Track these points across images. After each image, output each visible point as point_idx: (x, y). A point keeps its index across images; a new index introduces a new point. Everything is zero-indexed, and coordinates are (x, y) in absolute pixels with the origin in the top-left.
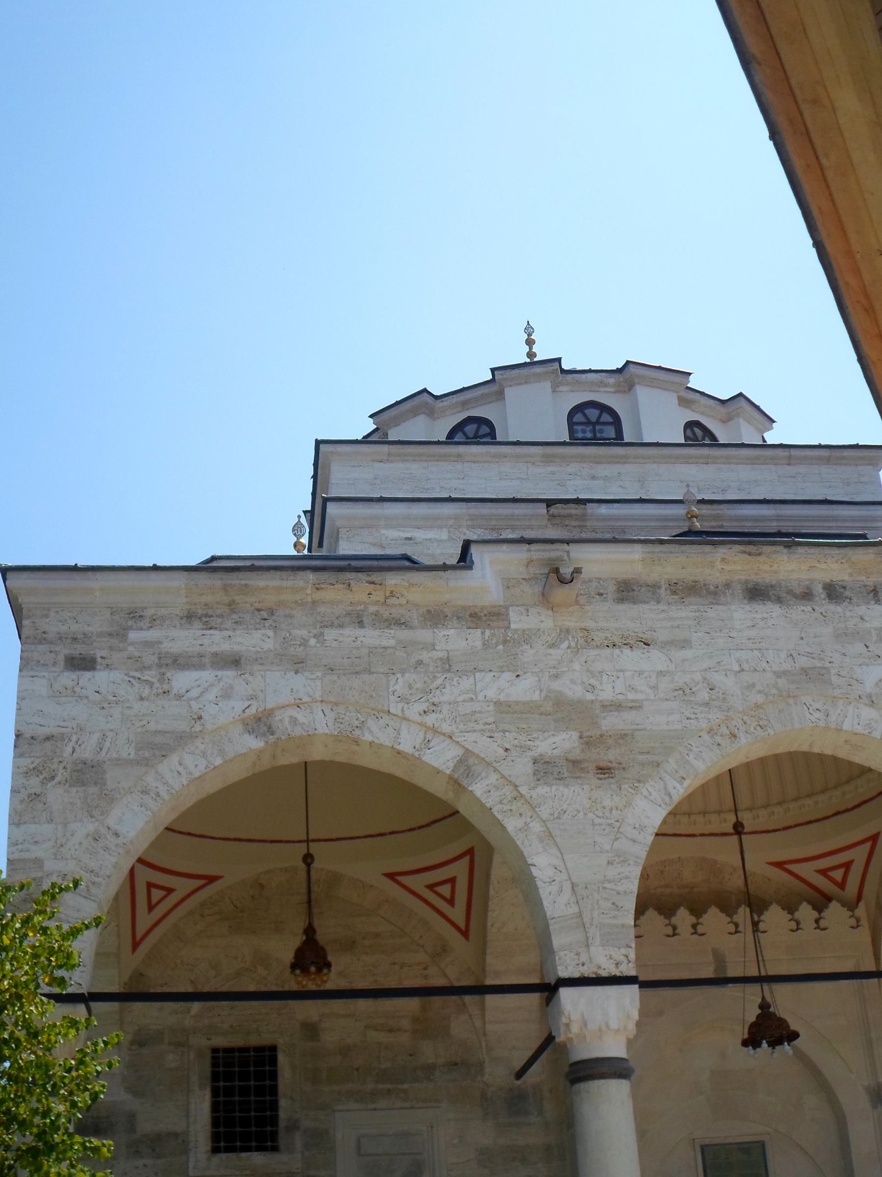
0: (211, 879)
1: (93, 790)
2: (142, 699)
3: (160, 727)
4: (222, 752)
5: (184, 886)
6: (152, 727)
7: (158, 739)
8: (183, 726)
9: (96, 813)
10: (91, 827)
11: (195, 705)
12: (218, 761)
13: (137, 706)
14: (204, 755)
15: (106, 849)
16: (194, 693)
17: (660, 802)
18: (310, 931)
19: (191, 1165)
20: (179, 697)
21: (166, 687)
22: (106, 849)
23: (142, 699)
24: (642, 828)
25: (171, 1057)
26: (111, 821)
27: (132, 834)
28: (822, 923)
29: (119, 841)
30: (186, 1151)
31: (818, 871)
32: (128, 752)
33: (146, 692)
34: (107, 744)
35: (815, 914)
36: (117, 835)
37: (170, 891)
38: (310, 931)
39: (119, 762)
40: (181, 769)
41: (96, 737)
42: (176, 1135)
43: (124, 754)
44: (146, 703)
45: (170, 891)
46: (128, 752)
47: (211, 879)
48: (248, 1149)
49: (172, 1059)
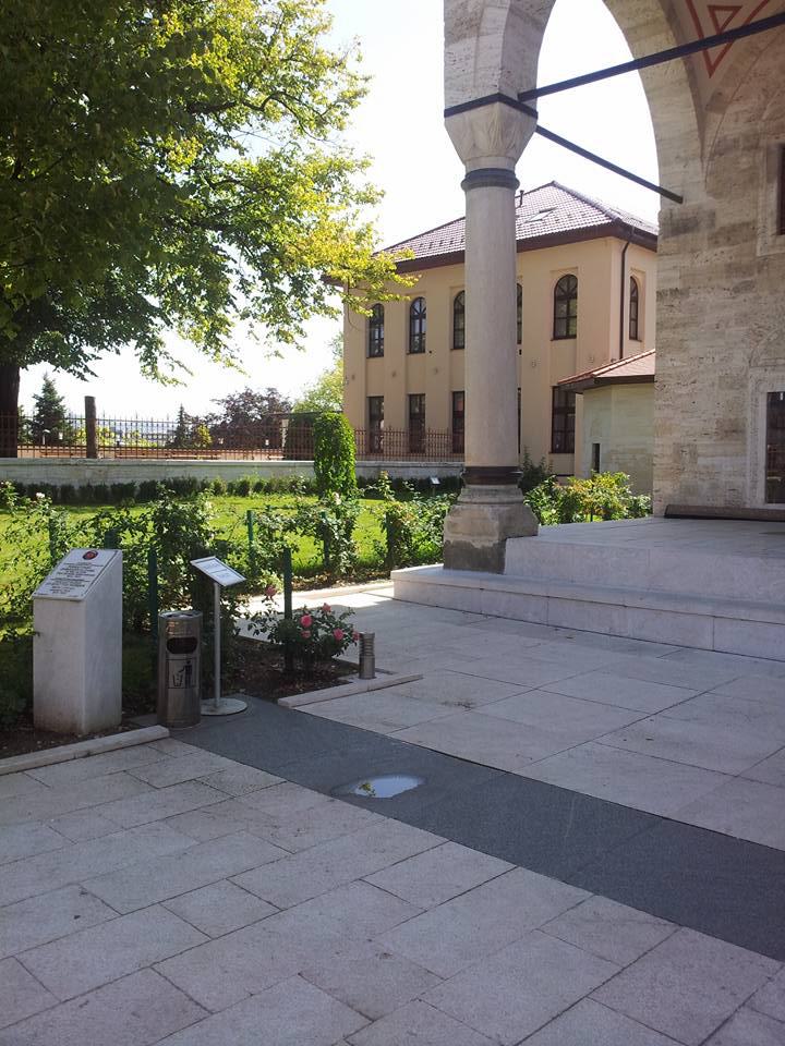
19: (758, 248)
25: (744, 160)
30: (754, 236)
42: (748, 224)
49: (745, 162)
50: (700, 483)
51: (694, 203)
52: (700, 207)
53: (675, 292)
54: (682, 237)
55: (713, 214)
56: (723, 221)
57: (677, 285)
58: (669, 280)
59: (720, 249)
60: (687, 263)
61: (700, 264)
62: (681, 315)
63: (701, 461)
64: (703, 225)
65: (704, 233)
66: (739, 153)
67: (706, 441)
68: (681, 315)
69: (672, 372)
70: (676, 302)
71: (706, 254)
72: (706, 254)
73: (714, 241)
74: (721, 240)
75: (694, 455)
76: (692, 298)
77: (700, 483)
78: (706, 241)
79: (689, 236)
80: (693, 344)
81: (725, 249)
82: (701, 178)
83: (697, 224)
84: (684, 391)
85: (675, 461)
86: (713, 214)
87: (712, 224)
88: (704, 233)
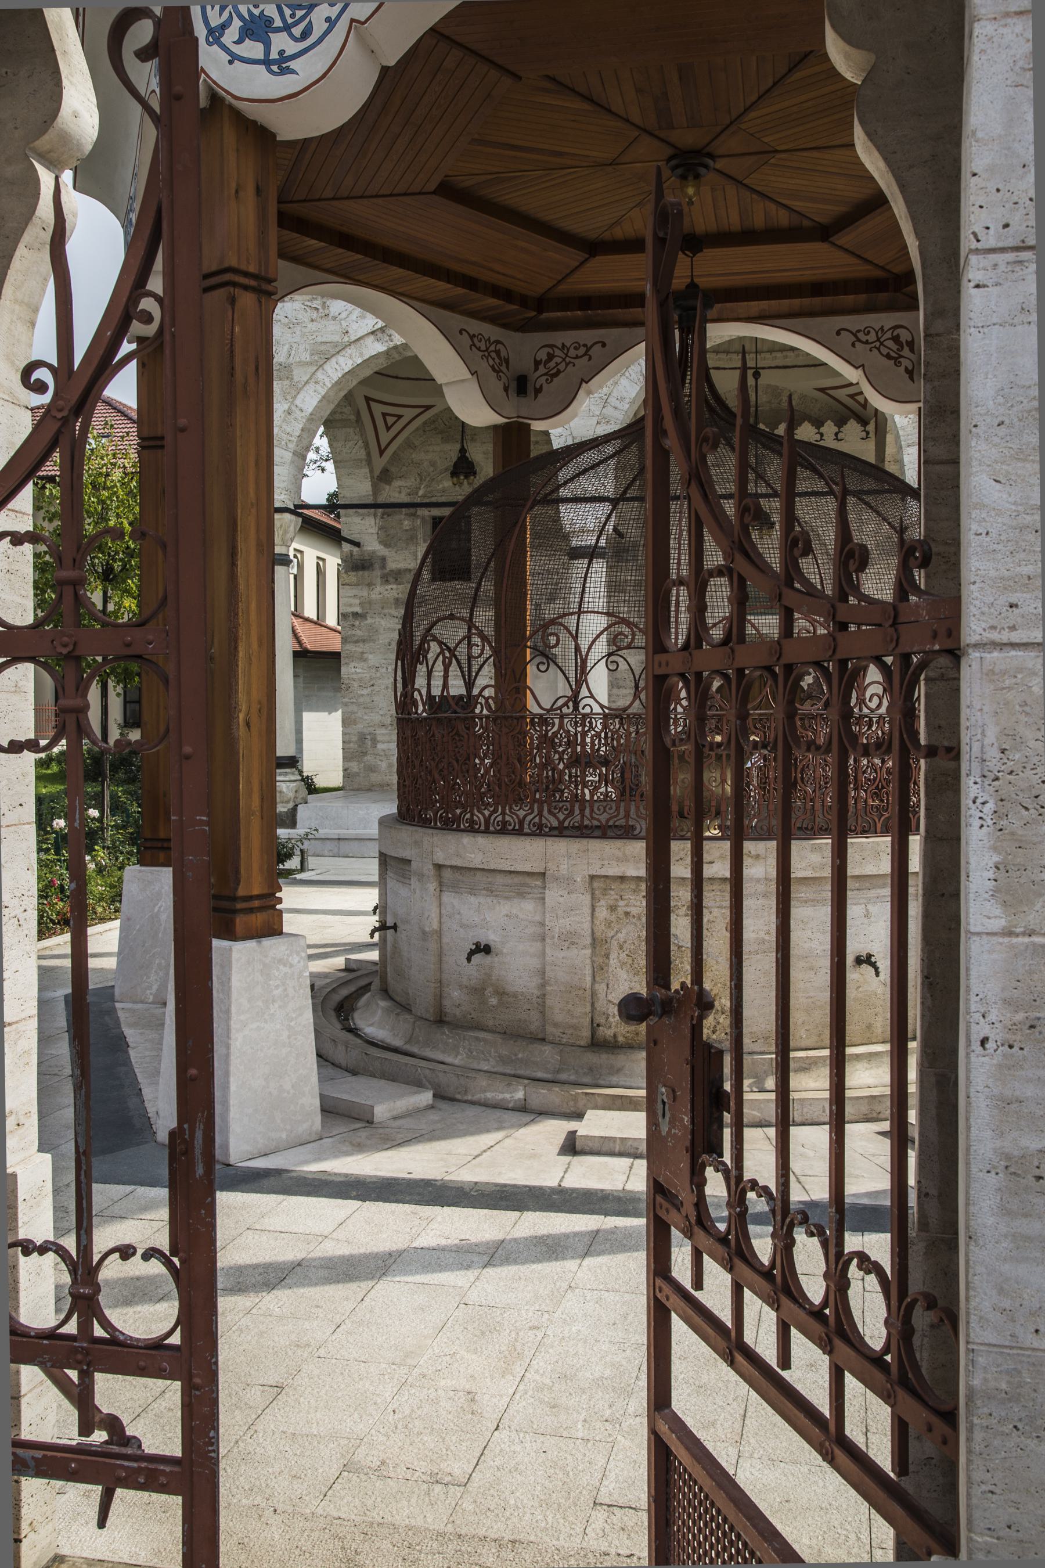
0: (428, 408)
1: (287, 382)
2: (312, 320)
3: (323, 340)
4: (361, 354)
5: (408, 414)
6: (319, 339)
7: (323, 348)
8: (336, 338)
9: (289, 397)
10: (286, 407)
11: (344, 324)
12: (359, 361)
13: (310, 325)
14: (351, 357)
15: (296, 419)
16: (343, 315)
17: (636, 380)
18: (463, 450)
20: (334, 318)
21: (326, 312)
22: (296, 419)
23: (312, 320)
24: (622, 399)
25: (406, 522)
26: (298, 402)
27: (310, 410)
28: (840, 436)
29: (303, 414)
31: (848, 396)
32: (305, 357)
33: (315, 315)
34: (293, 352)
35: (836, 429)
36: (301, 410)
37: (400, 417)
38: (463, 450)
39: (302, 364)
40: (337, 367)
41: (287, 347)
43: (303, 359)
44: (315, 323)
45: (400, 417)
46: (305, 357)
47: (428, 408)
48: (453, 579)
49: (407, 523)
50: (379, 763)
51: (370, 548)
52: (374, 552)
53: (355, 615)
54: (361, 573)
55: (384, 559)
56: (392, 565)
57: (358, 609)
58: (351, 605)
59: (390, 586)
60: (365, 593)
61: (375, 596)
62: (359, 633)
63: (380, 746)
64: (377, 566)
65: (378, 573)
66: (403, 517)
67: (383, 731)
68: (359, 633)
69: (355, 676)
70: (357, 623)
71: (379, 588)
72: (379, 588)
73: (385, 579)
74: (391, 579)
75: (375, 741)
76: (369, 621)
77: (379, 763)
78: (379, 579)
79: (366, 573)
80: (371, 656)
81: (394, 587)
82: (374, 530)
83: (372, 565)
84: (365, 692)
85: (360, 746)
86: (384, 559)
87: (383, 567)
88: (378, 573)
